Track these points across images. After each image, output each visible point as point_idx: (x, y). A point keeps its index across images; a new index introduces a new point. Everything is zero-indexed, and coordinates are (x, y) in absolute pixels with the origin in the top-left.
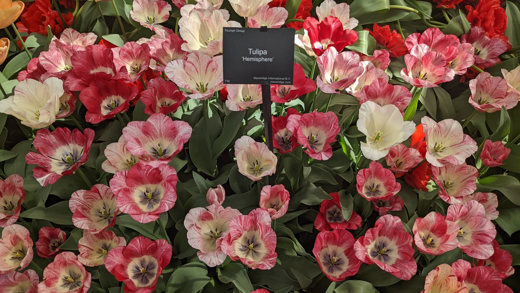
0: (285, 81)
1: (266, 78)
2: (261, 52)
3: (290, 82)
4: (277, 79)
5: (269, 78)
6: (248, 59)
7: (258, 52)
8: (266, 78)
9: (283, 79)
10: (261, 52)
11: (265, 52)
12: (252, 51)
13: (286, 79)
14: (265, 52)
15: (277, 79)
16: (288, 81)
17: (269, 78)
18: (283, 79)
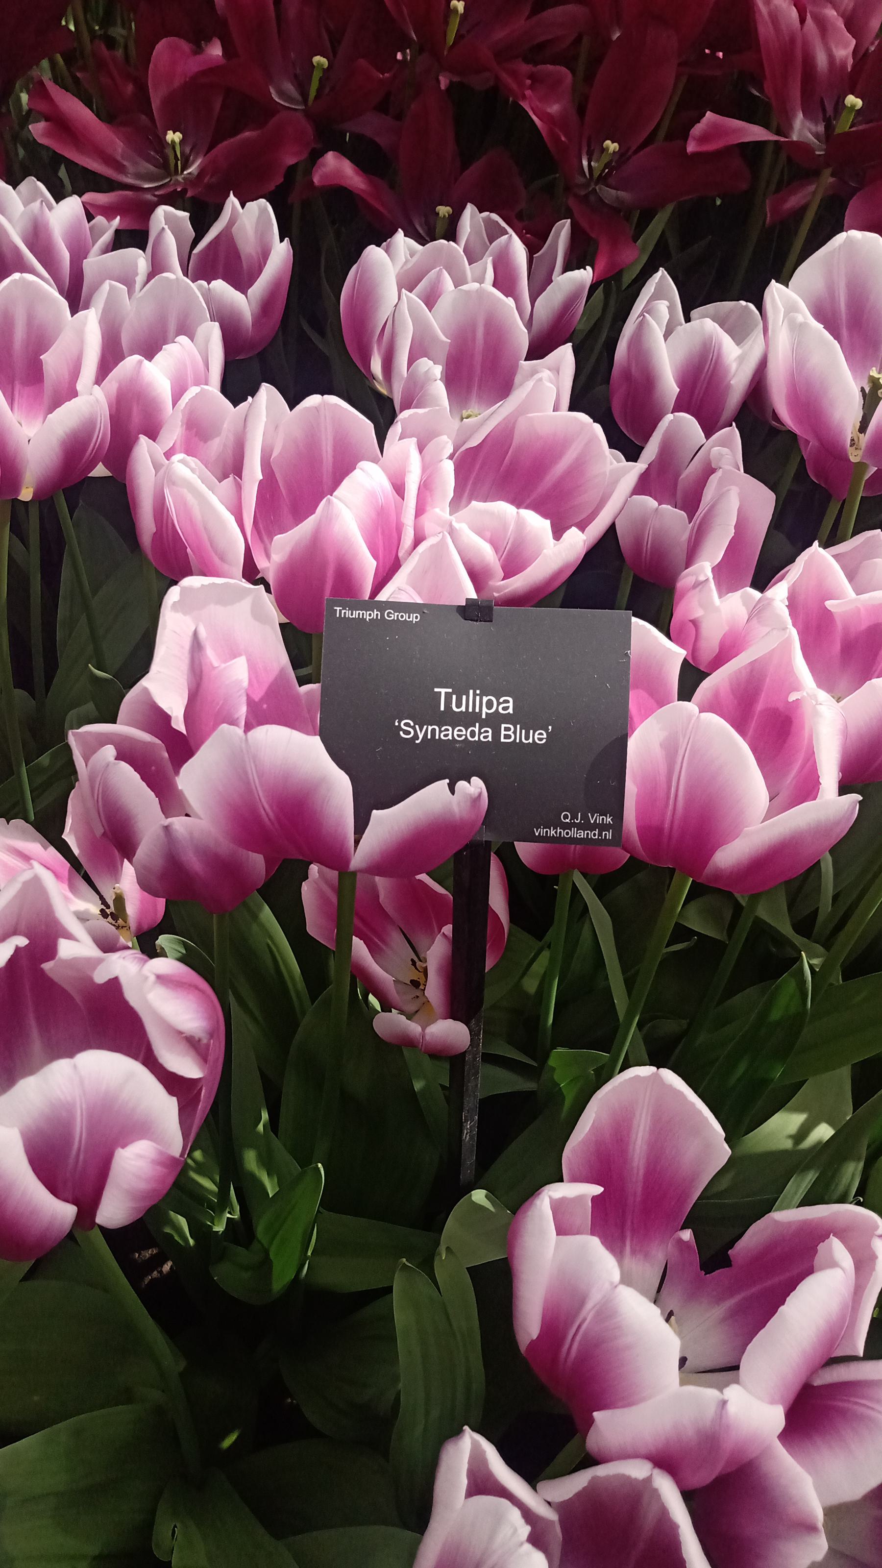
2: (489, 705)
7: (475, 702)
10: (489, 705)
11: (507, 705)
12: (448, 696)
14: (507, 705)
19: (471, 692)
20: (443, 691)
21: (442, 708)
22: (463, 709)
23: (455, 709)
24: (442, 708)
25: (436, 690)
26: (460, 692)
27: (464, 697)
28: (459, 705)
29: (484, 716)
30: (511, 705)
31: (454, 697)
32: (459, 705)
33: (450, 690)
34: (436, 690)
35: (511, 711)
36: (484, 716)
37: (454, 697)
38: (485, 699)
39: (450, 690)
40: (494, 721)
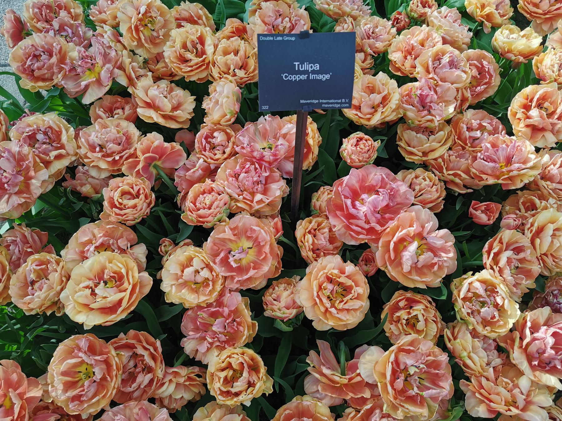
0: (341, 103)
1: (317, 101)
2: (311, 67)
3: (348, 105)
4: (331, 101)
5: (321, 101)
6: (293, 78)
8: (317, 101)
9: (340, 101)
10: (311, 67)
11: (317, 67)
12: (298, 65)
13: (343, 101)
14: (317, 67)
15: (331, 101)
16: (345, 103)
17: (321, 101)
18: (340, 101)
20: (297, 63)
21: (297, 69)
23: (301, 69)
24: (297, 69)
26: (302, 63)
28: (302, 68)
30: (318, 67)
32: (302, 68)
35: (318, 69)
38: (310, 65)
40: (314, 72)
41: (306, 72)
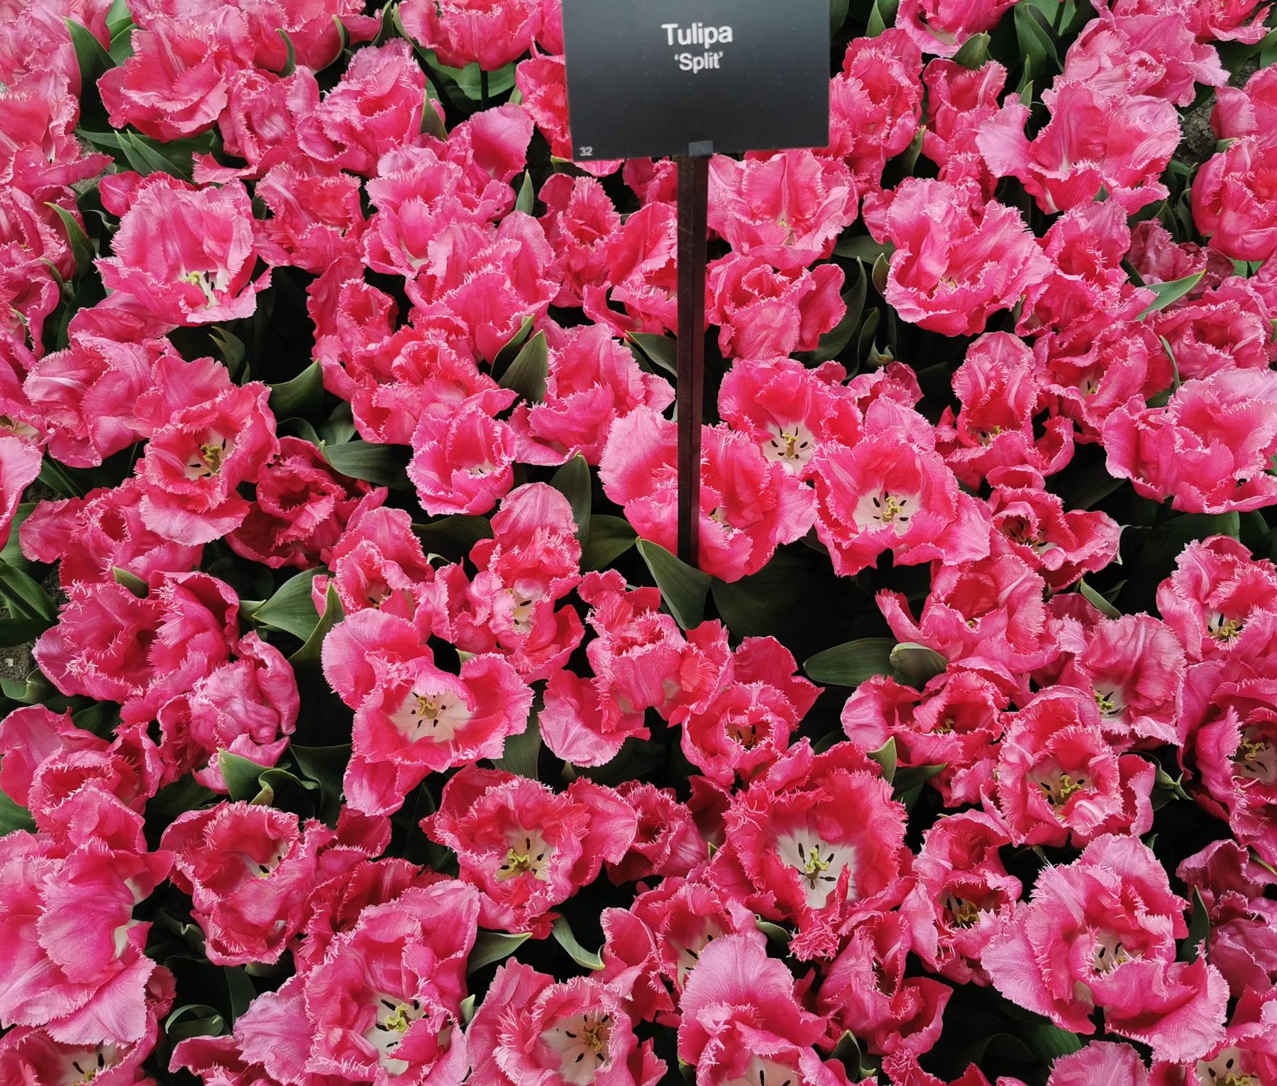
7: (698, 34)
11: (726, 35)
12: (675, 31)
19: (694, 25)
20: (670, 27)
21: (671, 42)
22: (688, 41)
24: (671, 42)
25: (664, 26)
26: (685, 26)
27: (688, 31)
28: (685, 38)
29: (707, 46)
31: (680, 32)
32: (685, 38)
33: (676, 26)
34: (664, 26)
36: (707, 46)
37: (680, 32)
38: (707, 30)
39: (676, 26)
41: (697, 50)
